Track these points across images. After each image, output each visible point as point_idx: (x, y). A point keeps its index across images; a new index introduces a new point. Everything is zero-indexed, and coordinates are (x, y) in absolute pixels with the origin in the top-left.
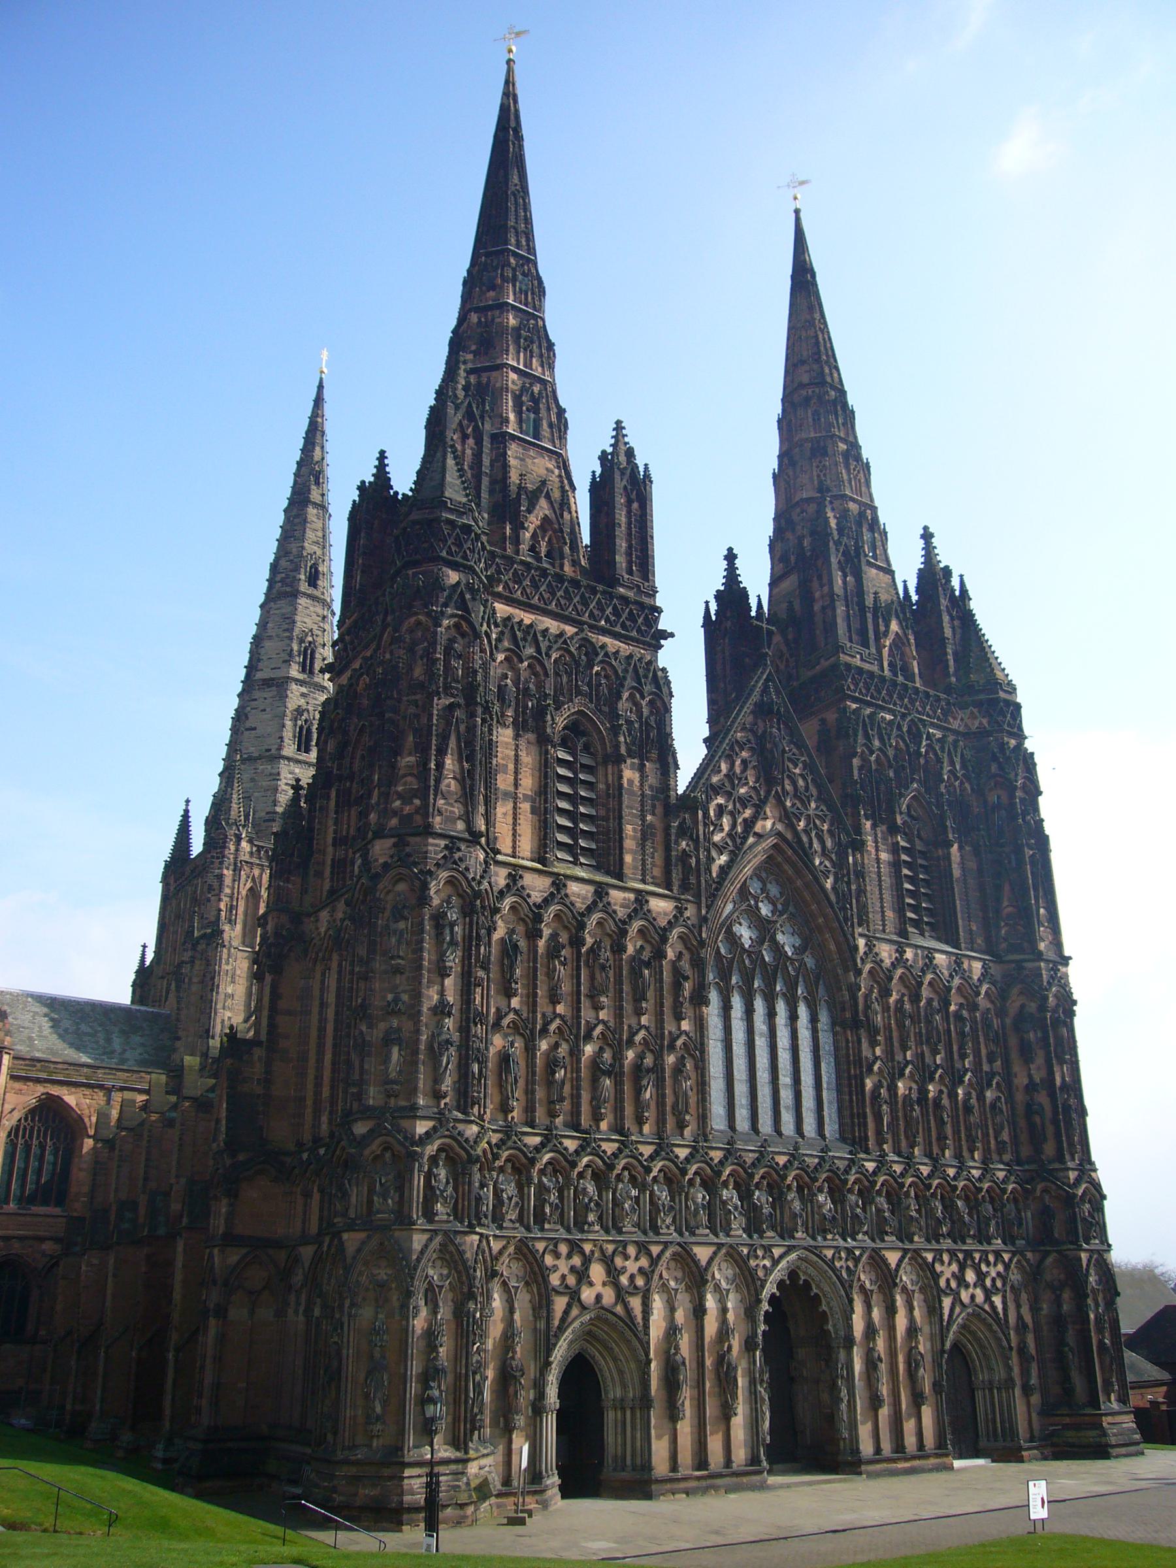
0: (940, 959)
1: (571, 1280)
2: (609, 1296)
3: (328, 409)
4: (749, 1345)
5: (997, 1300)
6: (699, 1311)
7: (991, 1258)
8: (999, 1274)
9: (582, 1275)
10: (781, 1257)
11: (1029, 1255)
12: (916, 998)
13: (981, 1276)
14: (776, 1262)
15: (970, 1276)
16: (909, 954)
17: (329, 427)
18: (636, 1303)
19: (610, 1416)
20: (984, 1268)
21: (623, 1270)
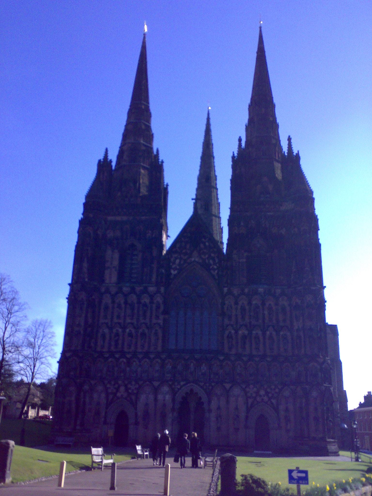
0: (261, 290)
1: (115, 391)
2: (125, 395)
3: (212, 121)
4: (173, 410)
5: (274, 401)
6: (156, 400)
7: (273, 387)
8: (276, 393)
9: (118, 390)
10: (184, 385)
11: (292, 387)
12: (250, 303)
13: (267, 393)
14: (181, 387)
15: (262, 392)
16: (246, 290)
17: (212, 128)
18: (133, 397)
19: (131, 428)
20: (269, 390)
21: (130, 389)
